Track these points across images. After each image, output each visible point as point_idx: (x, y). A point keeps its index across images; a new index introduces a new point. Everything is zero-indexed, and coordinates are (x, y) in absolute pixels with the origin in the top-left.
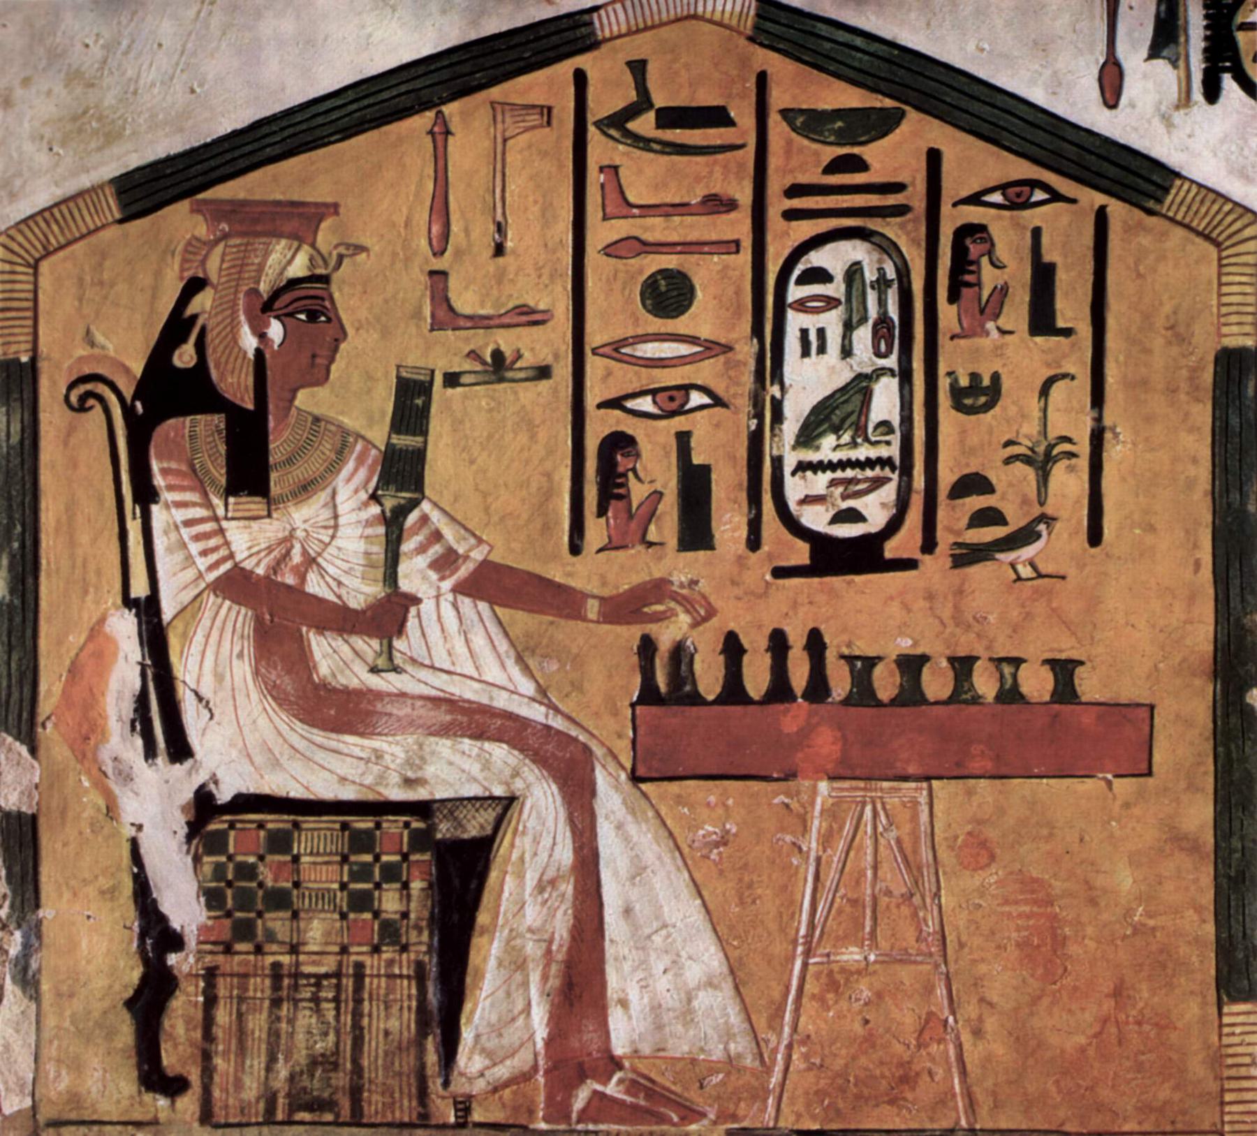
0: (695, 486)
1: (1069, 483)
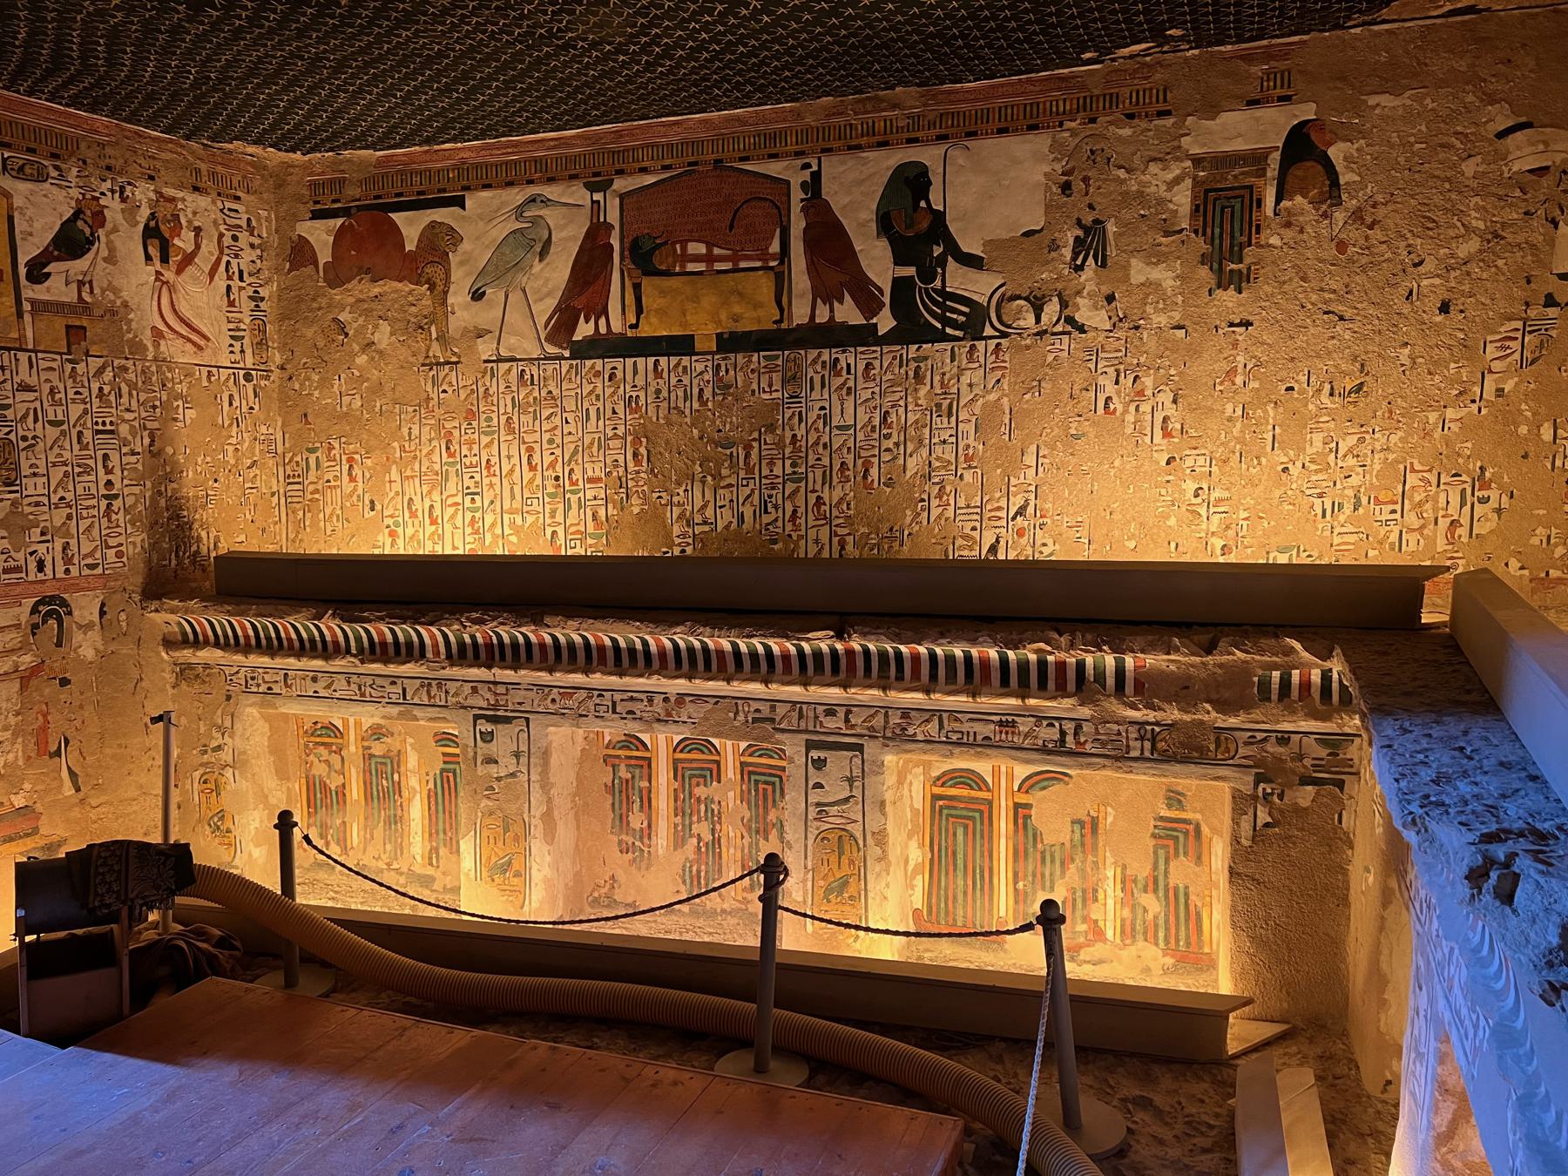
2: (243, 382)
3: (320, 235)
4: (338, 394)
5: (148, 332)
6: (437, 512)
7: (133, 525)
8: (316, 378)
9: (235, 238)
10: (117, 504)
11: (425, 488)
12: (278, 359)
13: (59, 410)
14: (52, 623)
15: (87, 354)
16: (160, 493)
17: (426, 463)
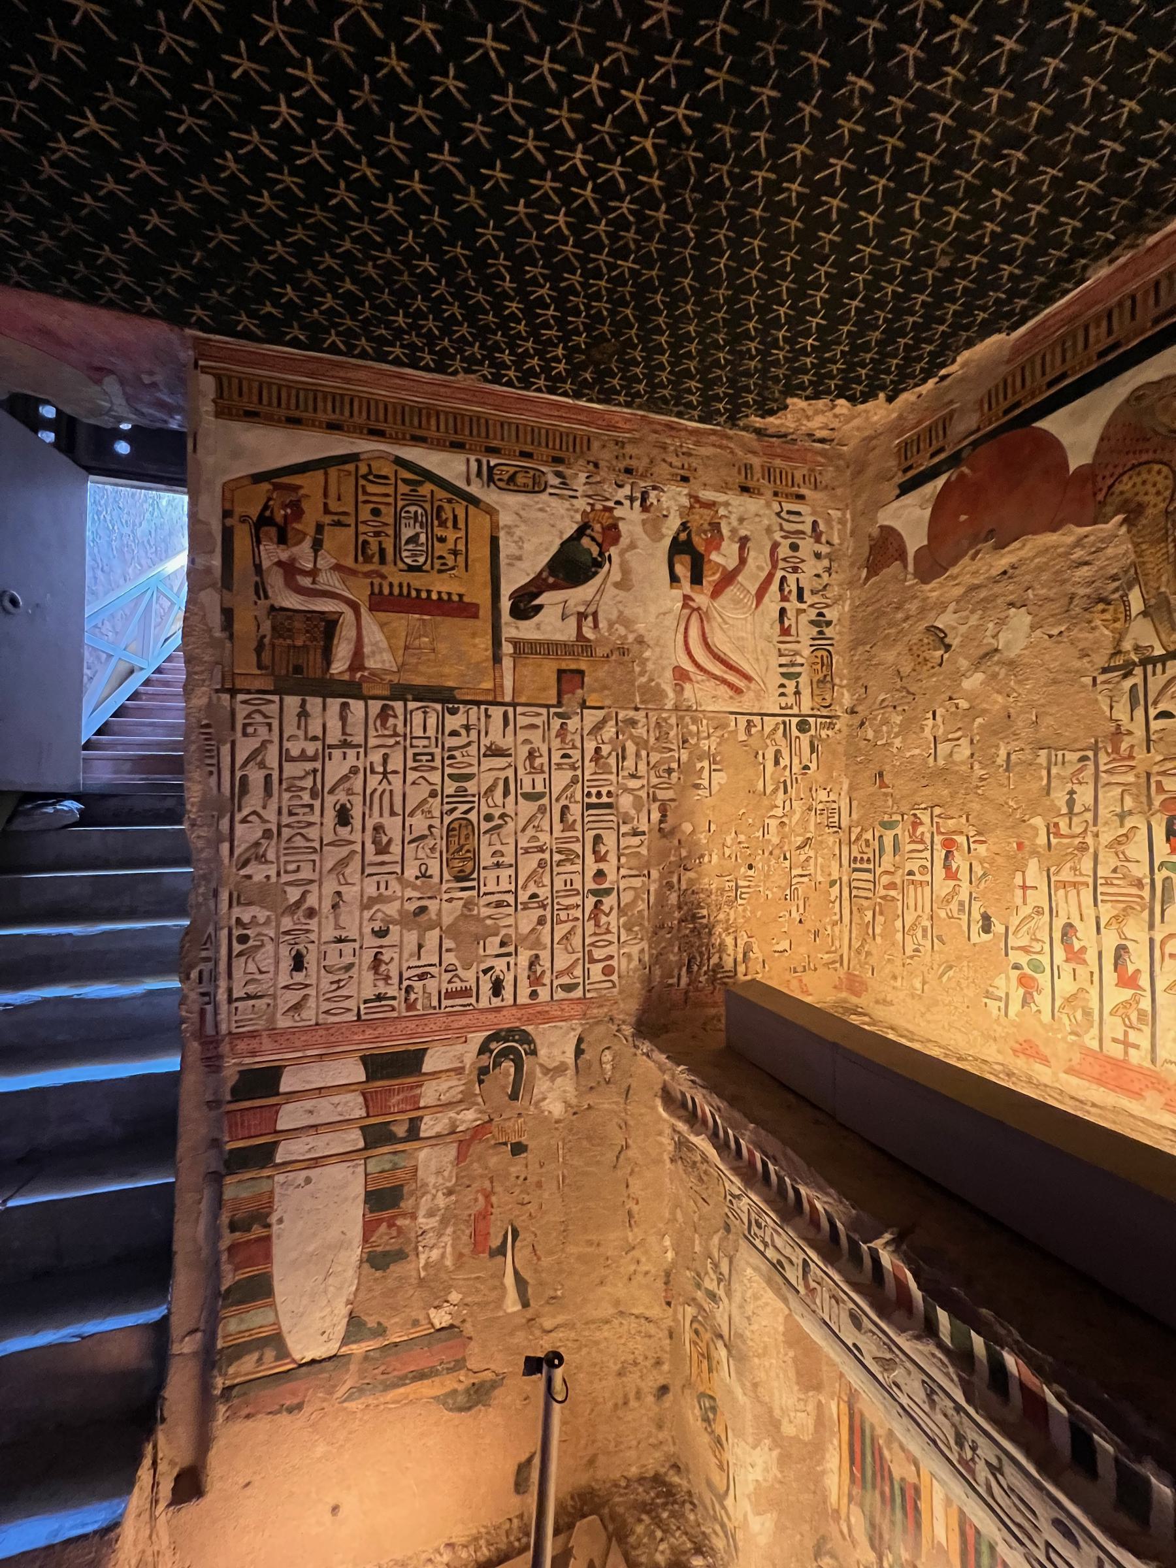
0: (382, 551)
1: (461, 559)
2: (795, 732)
3: (910, 517)
4: (930, 739)
5: (669, 674)
6: (1138, 961)
7: (629, 930)
8: (898, 719)
9: (794, 547)
10: (609, 902)
11: (1106, 911)
12: (847, 700)
13: (539, 780)
14: (508, 1066)
15: (583, 705)
16: (670, 886)
17: (1108, 861)
